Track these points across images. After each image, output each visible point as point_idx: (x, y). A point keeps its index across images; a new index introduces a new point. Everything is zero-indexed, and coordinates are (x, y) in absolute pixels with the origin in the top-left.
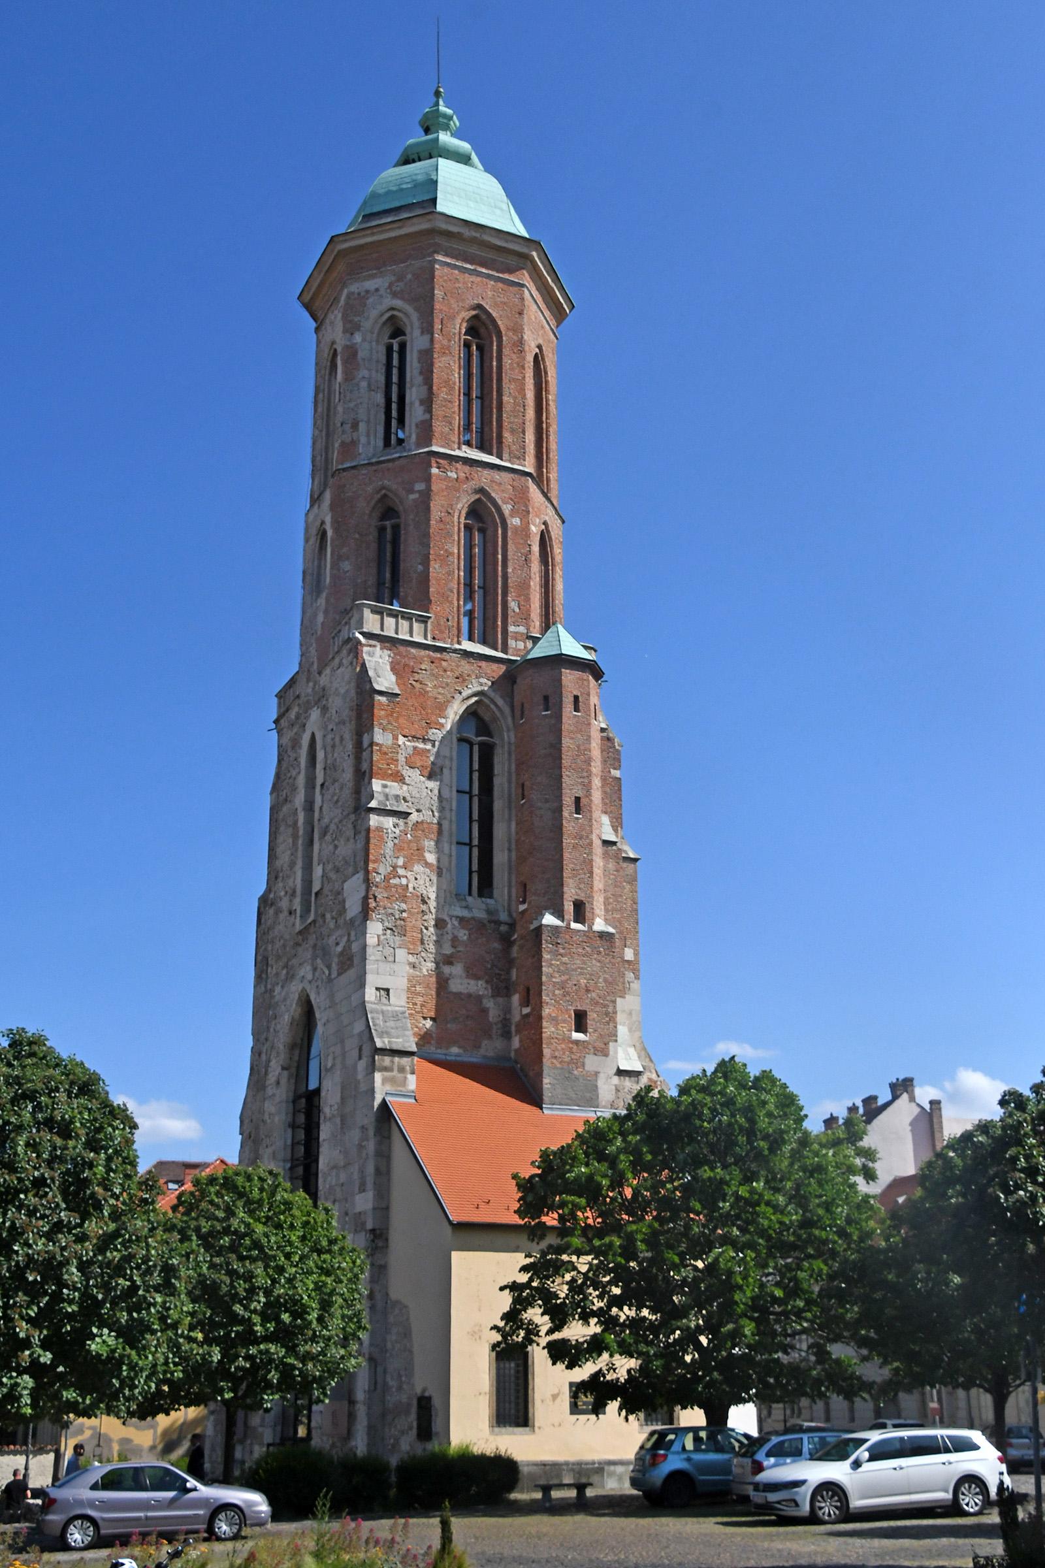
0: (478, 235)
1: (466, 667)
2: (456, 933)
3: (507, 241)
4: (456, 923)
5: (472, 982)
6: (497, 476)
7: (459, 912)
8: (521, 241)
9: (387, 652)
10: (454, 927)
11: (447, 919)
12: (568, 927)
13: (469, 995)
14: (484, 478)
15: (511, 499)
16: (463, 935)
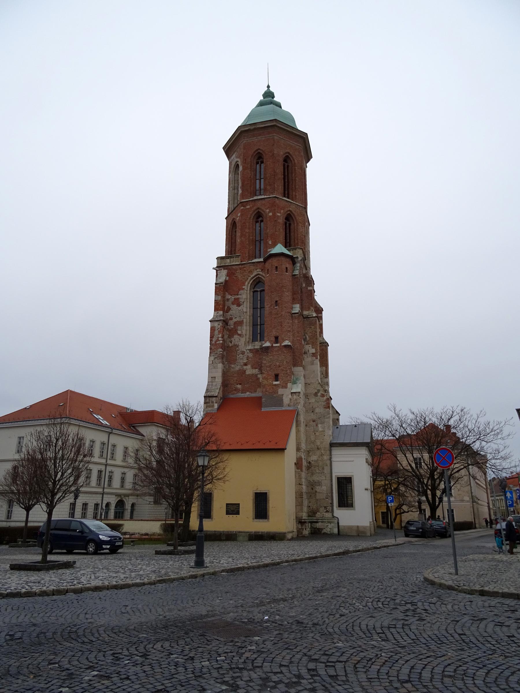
0: (255, 127)
1: (252, 267)
2: (248, 354)
3: (265, 124)
4: (248, 351)
5: (254, 370)
6: (263, 202)
7: (250, 347)
8: (269, 122)
9: (225, 270)
10: (248, 353)
11: (245, 351)
12: (272, 346)
13: (253, 374)
14: (259, 204)
15: (269, 207)
16: (251, 355)
